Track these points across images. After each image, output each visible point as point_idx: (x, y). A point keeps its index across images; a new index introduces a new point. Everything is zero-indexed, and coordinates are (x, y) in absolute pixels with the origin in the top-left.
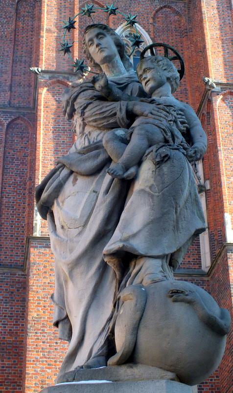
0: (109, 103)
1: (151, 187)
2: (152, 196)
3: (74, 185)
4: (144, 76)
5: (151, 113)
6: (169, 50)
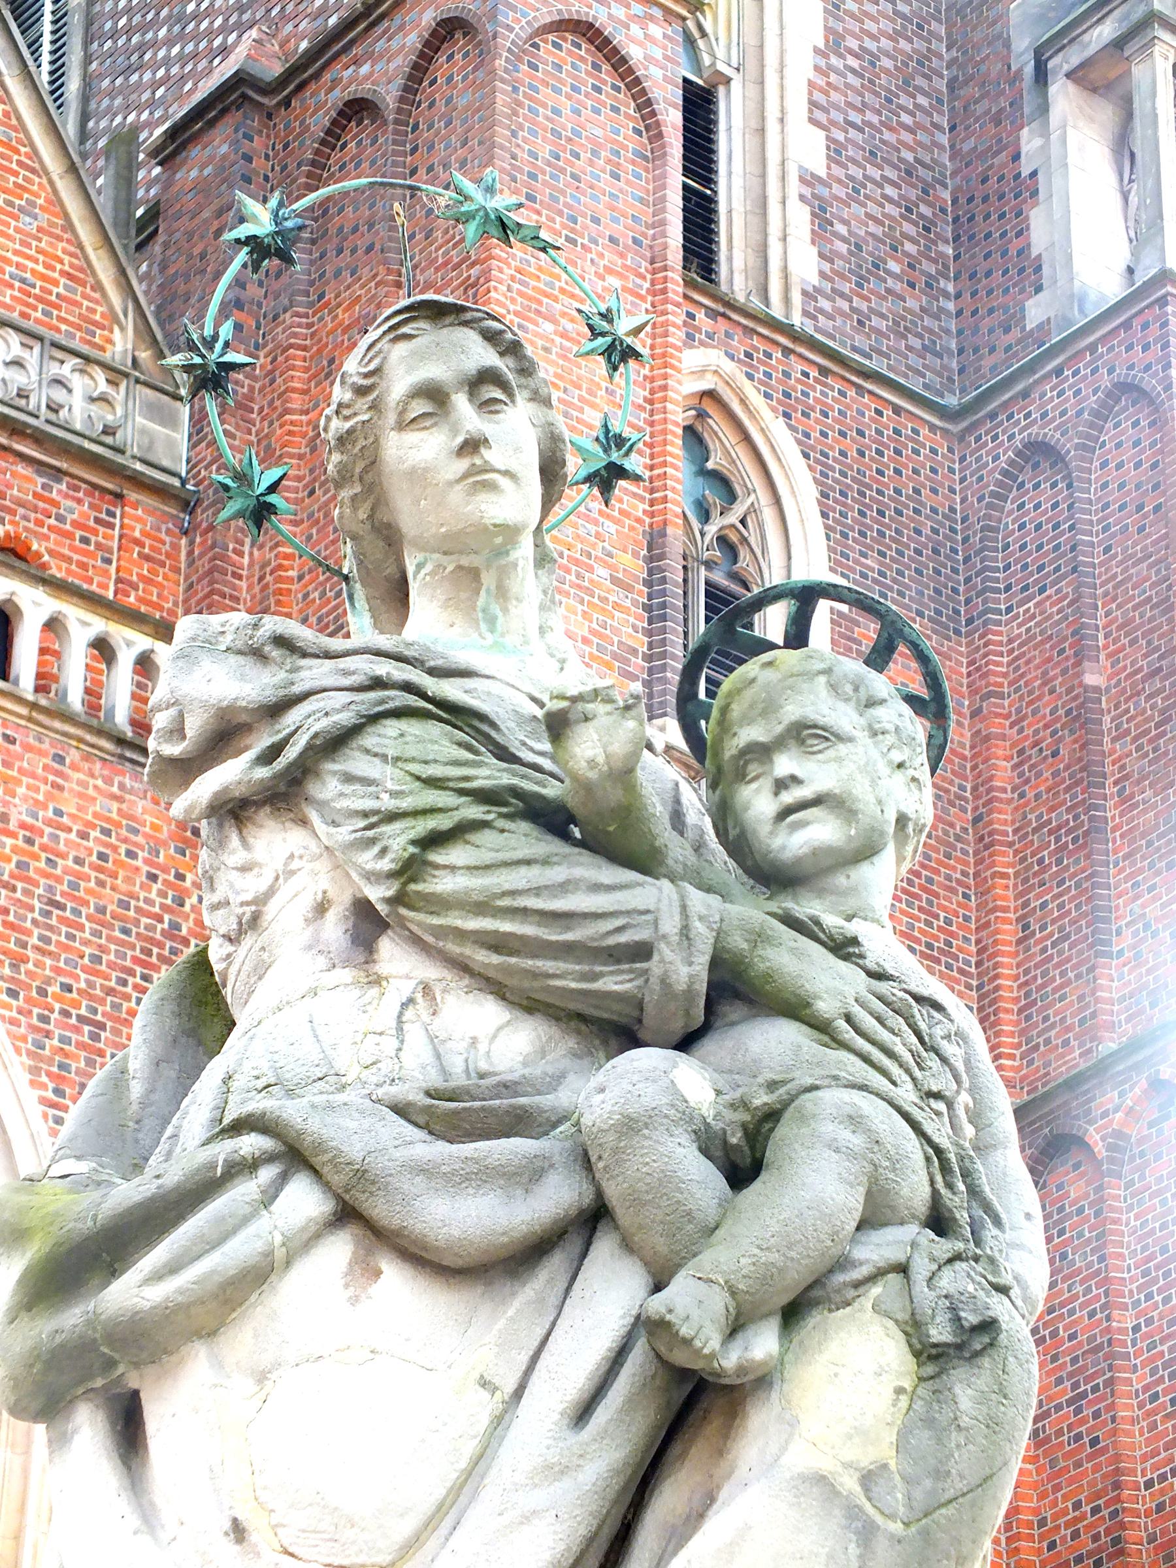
0: (611, 874)
1: (868, 1479)
2: (867, 1533)
3: (355, 1300)
4: (784, 764)
5: (849, 1019)
6: (902, 648)
